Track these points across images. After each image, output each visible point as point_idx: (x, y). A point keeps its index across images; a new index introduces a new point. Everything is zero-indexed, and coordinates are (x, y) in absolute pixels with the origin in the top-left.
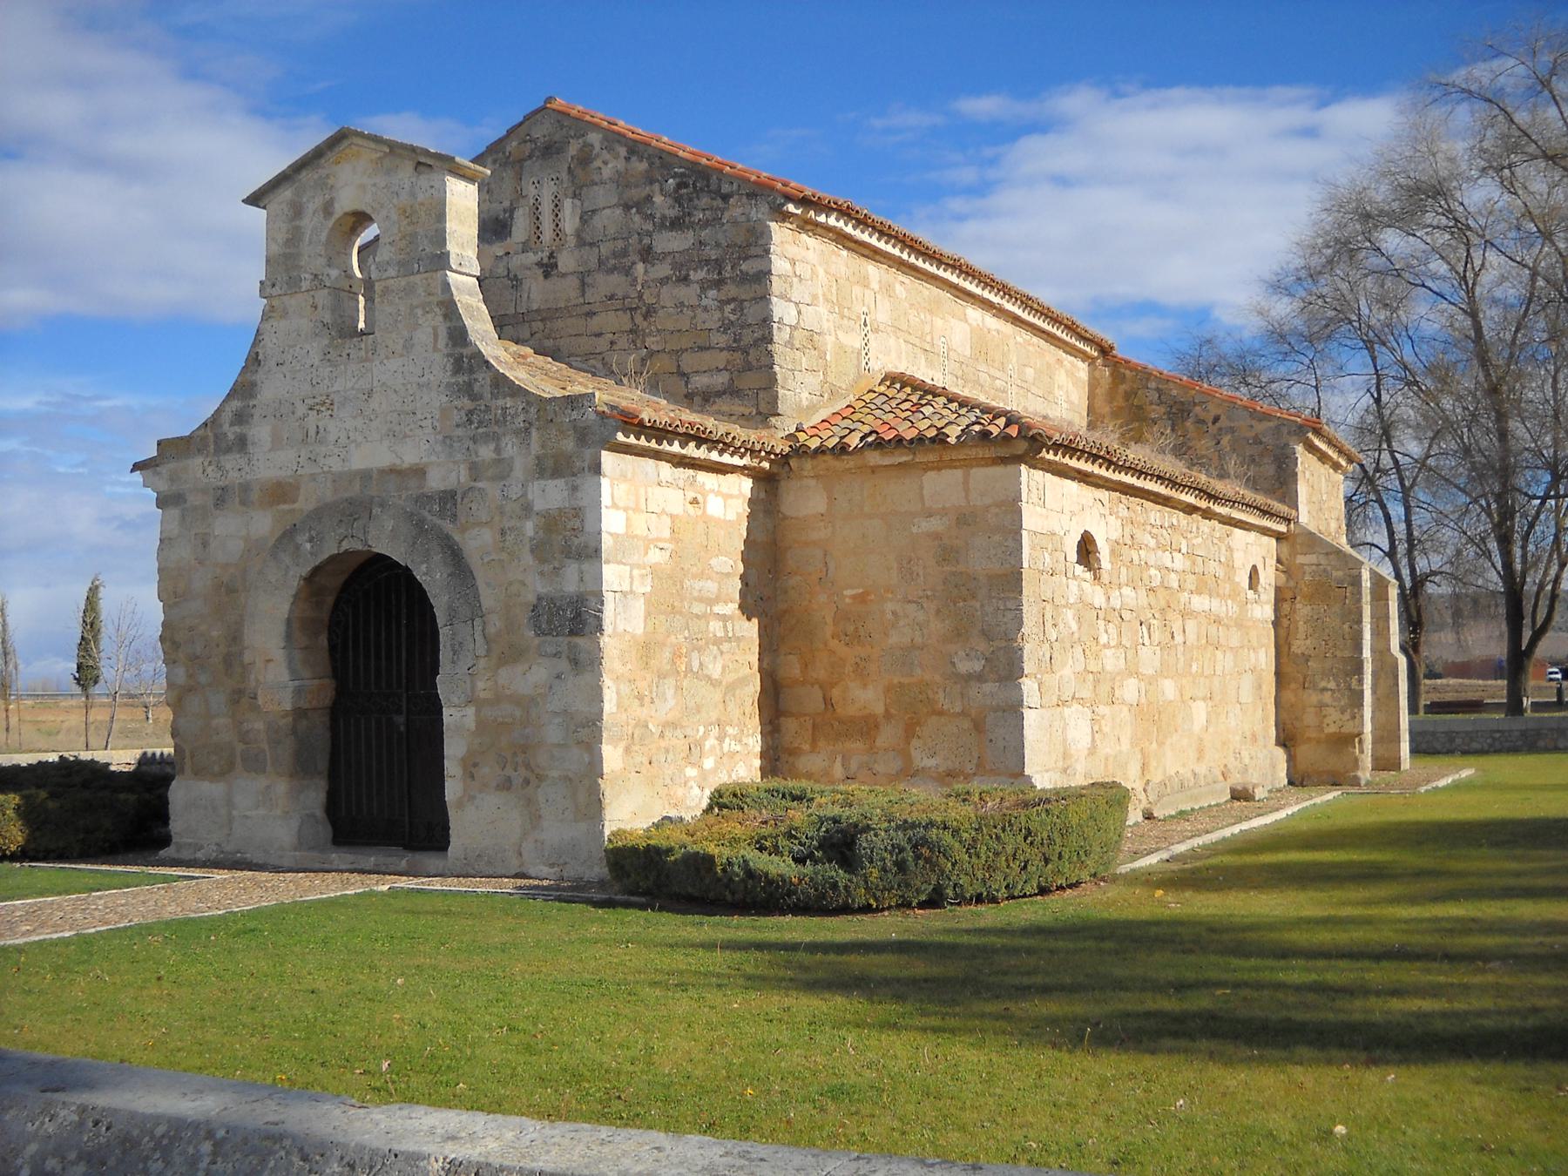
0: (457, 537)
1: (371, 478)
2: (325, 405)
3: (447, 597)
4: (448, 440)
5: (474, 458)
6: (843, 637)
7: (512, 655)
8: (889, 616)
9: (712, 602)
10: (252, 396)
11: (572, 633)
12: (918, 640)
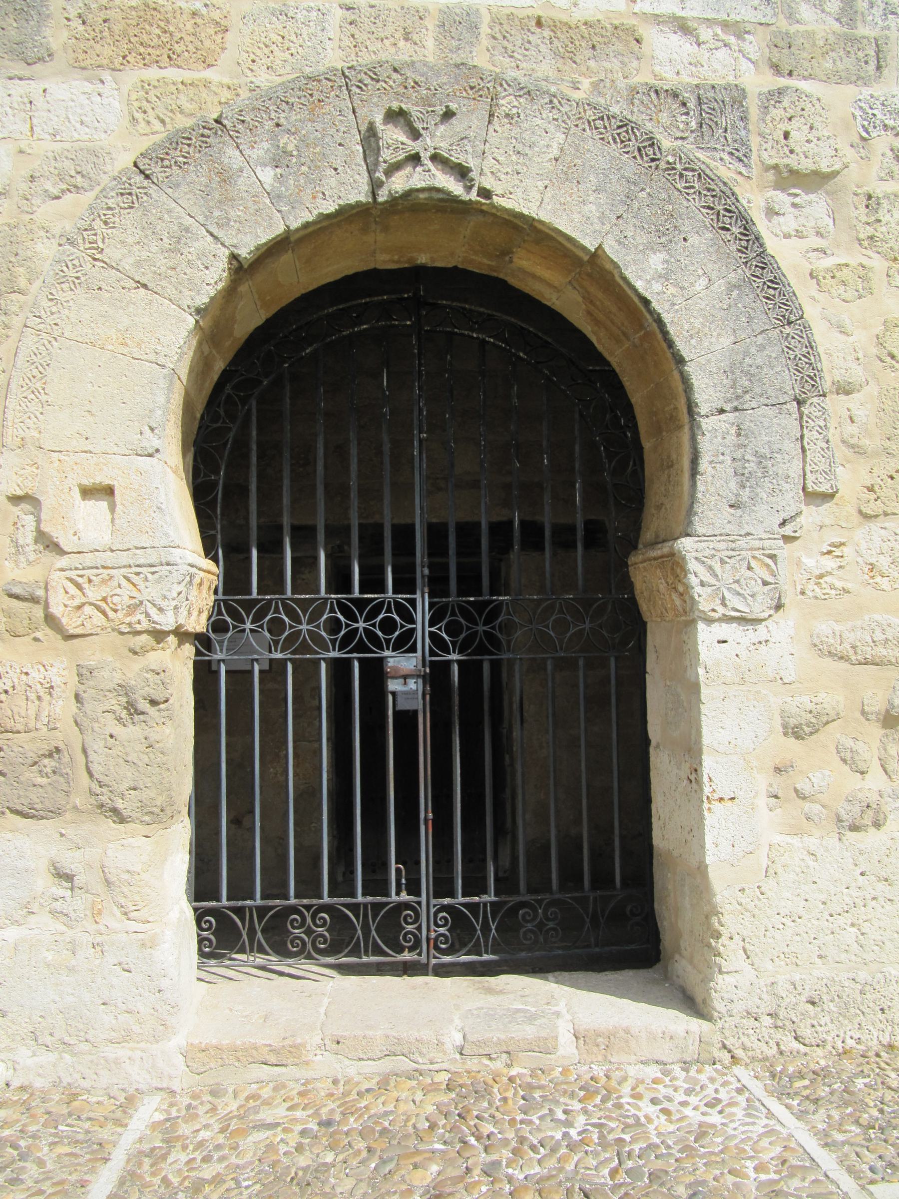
1: (474, 28)
3: (726, 341)
5: (782, 23)
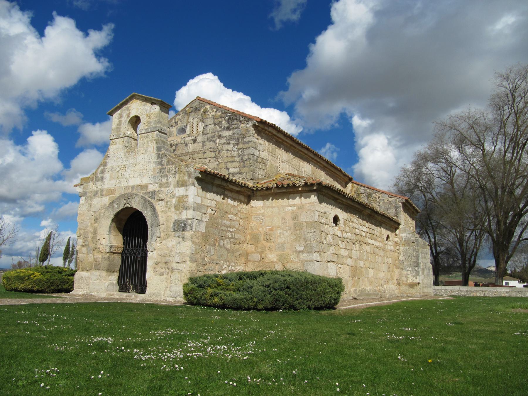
0: (155, 204)
2: (124, 168)
4: (155, 177)
5: (161, 182)
6: (266, 240)
7: (167, 236)
8: (279, 234)
9: (227, 227)
10: (105, 166)
11: (183, 230)
12: (286, 241)
